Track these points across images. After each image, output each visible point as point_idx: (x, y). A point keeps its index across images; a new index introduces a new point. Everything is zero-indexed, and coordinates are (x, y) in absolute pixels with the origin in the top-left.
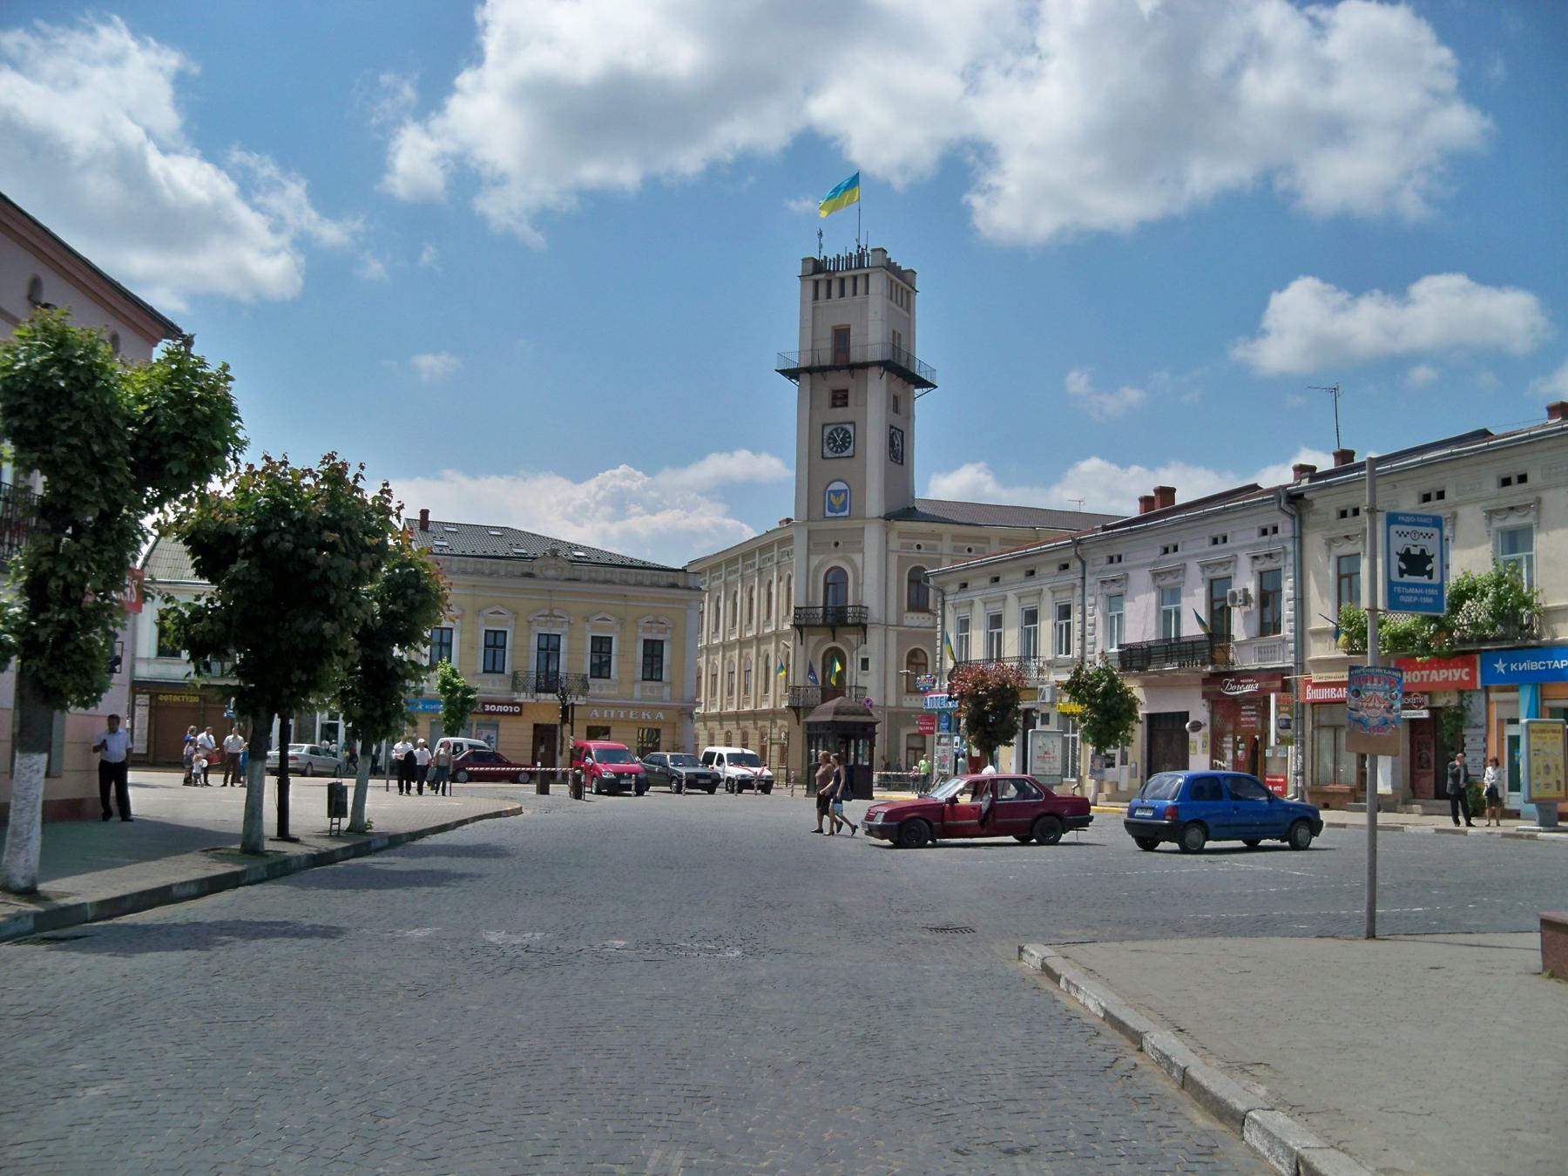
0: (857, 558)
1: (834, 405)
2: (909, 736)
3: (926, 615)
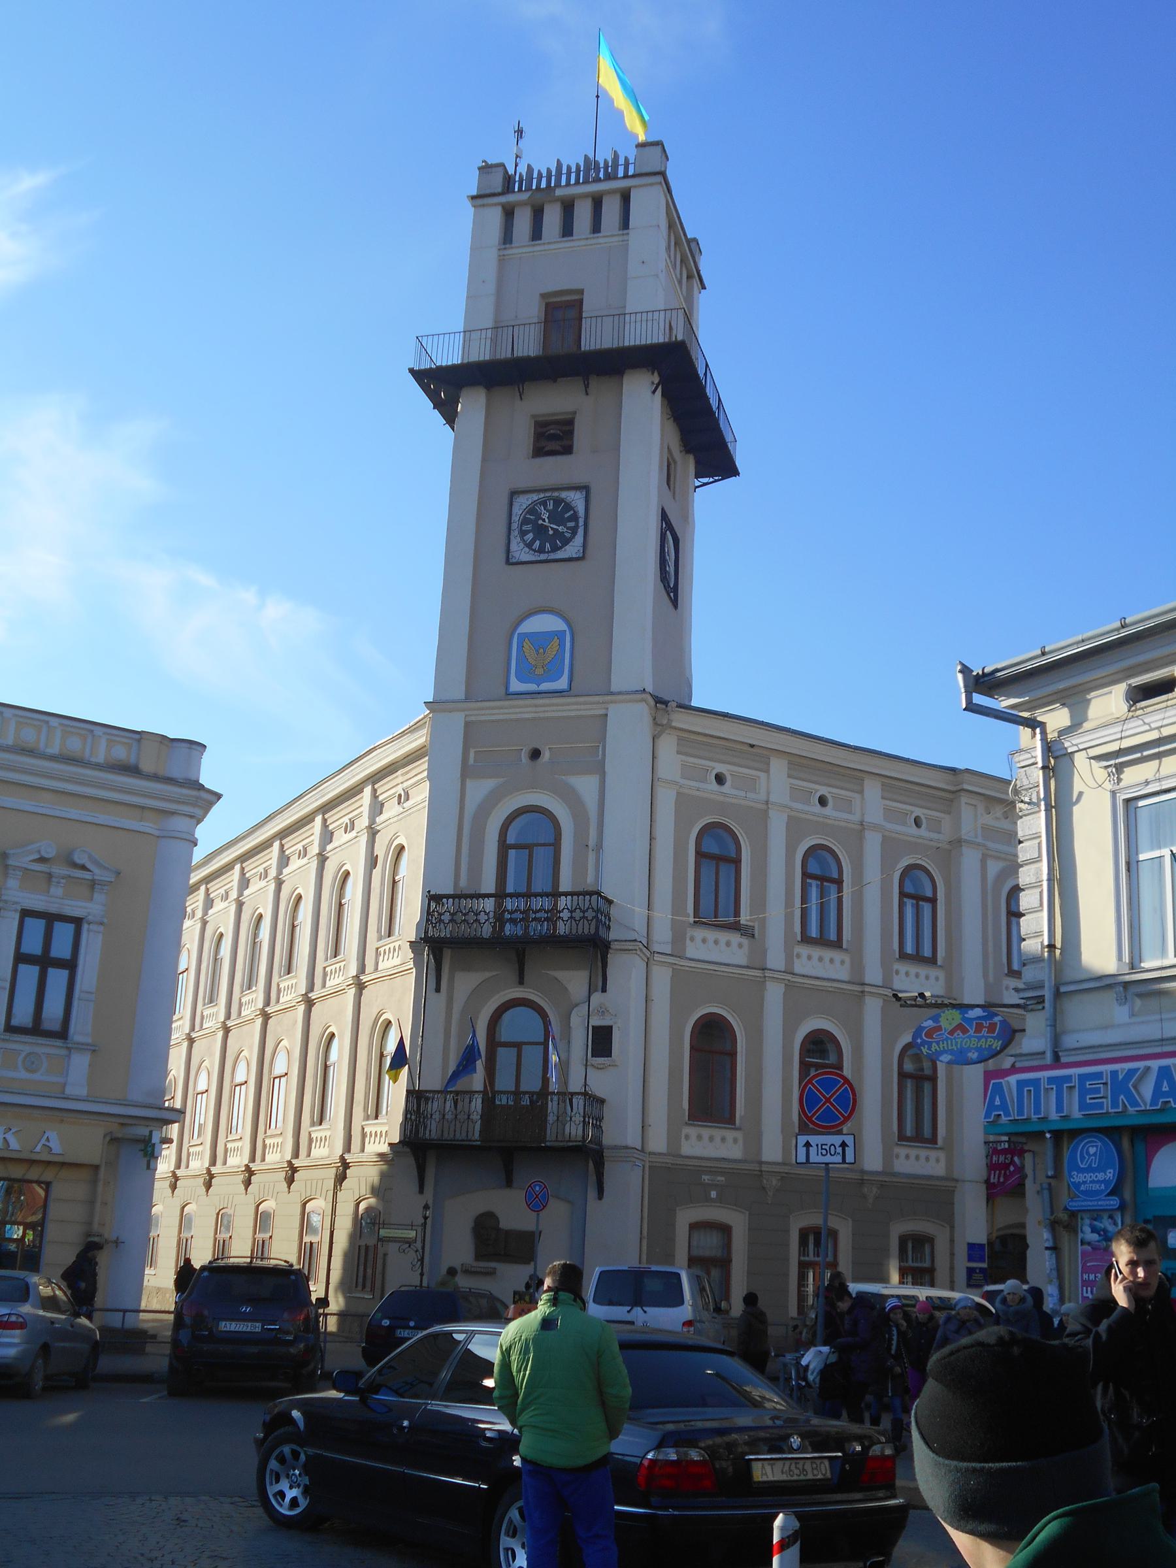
0: (586, 785)
1: (539, 452)
2: (694, 1227)
3: (735, 938)
